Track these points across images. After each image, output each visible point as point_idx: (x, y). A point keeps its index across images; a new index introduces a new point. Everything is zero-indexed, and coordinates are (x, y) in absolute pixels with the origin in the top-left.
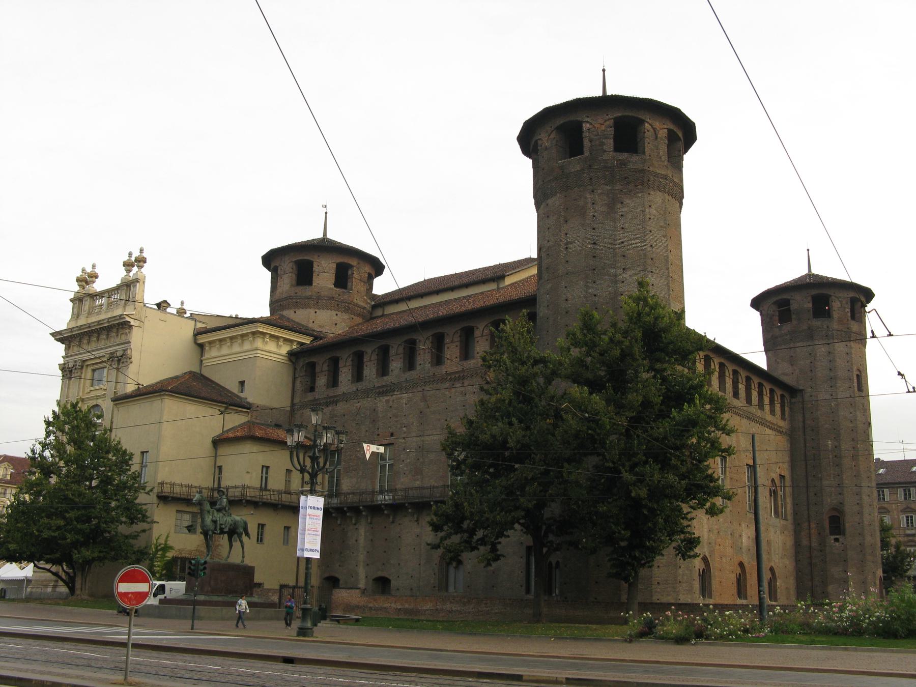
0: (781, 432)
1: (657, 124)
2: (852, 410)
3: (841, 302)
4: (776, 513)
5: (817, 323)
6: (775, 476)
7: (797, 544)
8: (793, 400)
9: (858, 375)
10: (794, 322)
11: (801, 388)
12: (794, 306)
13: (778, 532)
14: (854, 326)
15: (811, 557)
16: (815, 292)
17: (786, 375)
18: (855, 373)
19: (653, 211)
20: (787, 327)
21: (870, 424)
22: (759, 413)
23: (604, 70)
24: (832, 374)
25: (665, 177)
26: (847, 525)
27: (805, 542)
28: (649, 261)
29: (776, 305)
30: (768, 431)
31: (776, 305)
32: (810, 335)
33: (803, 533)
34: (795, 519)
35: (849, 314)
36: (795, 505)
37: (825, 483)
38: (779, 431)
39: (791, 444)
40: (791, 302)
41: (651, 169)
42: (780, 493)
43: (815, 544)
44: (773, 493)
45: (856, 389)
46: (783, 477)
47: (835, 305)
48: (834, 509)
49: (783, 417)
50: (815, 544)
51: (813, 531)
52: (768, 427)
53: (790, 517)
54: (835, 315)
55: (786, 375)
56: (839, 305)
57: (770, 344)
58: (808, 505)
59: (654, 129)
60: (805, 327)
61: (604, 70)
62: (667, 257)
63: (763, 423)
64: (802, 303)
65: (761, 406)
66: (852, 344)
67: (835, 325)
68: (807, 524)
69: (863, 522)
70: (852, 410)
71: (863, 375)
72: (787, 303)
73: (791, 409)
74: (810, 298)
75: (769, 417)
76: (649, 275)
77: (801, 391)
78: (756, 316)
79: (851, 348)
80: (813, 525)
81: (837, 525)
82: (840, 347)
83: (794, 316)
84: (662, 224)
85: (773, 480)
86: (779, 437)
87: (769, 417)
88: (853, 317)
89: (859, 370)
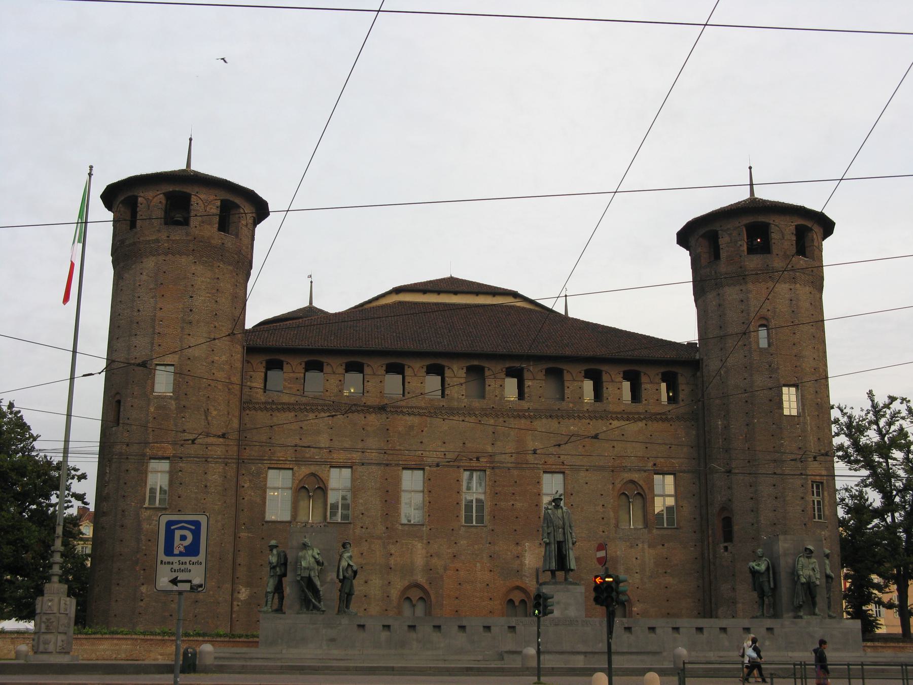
0: (667, 420)
1: (150, 194)
3: (730, 235)
6: (635, 476)
19: (144, 277)
23: (191, 139)
25: (157, 241)
28: (135, 325)
35: (745, 248)
41: (141, 239)
43: (711, 556)
47: (723, 241)
48: (723, 509)
52: (617, 419)
54: (723, 255)
59: (147, 200)
61: (191, 139)
62: (155, 316)
66: (750, 286)
70: (746, 375)
76: (133, 339)
80: (710, 532)
84: (151, 287)
85: (632, 482)
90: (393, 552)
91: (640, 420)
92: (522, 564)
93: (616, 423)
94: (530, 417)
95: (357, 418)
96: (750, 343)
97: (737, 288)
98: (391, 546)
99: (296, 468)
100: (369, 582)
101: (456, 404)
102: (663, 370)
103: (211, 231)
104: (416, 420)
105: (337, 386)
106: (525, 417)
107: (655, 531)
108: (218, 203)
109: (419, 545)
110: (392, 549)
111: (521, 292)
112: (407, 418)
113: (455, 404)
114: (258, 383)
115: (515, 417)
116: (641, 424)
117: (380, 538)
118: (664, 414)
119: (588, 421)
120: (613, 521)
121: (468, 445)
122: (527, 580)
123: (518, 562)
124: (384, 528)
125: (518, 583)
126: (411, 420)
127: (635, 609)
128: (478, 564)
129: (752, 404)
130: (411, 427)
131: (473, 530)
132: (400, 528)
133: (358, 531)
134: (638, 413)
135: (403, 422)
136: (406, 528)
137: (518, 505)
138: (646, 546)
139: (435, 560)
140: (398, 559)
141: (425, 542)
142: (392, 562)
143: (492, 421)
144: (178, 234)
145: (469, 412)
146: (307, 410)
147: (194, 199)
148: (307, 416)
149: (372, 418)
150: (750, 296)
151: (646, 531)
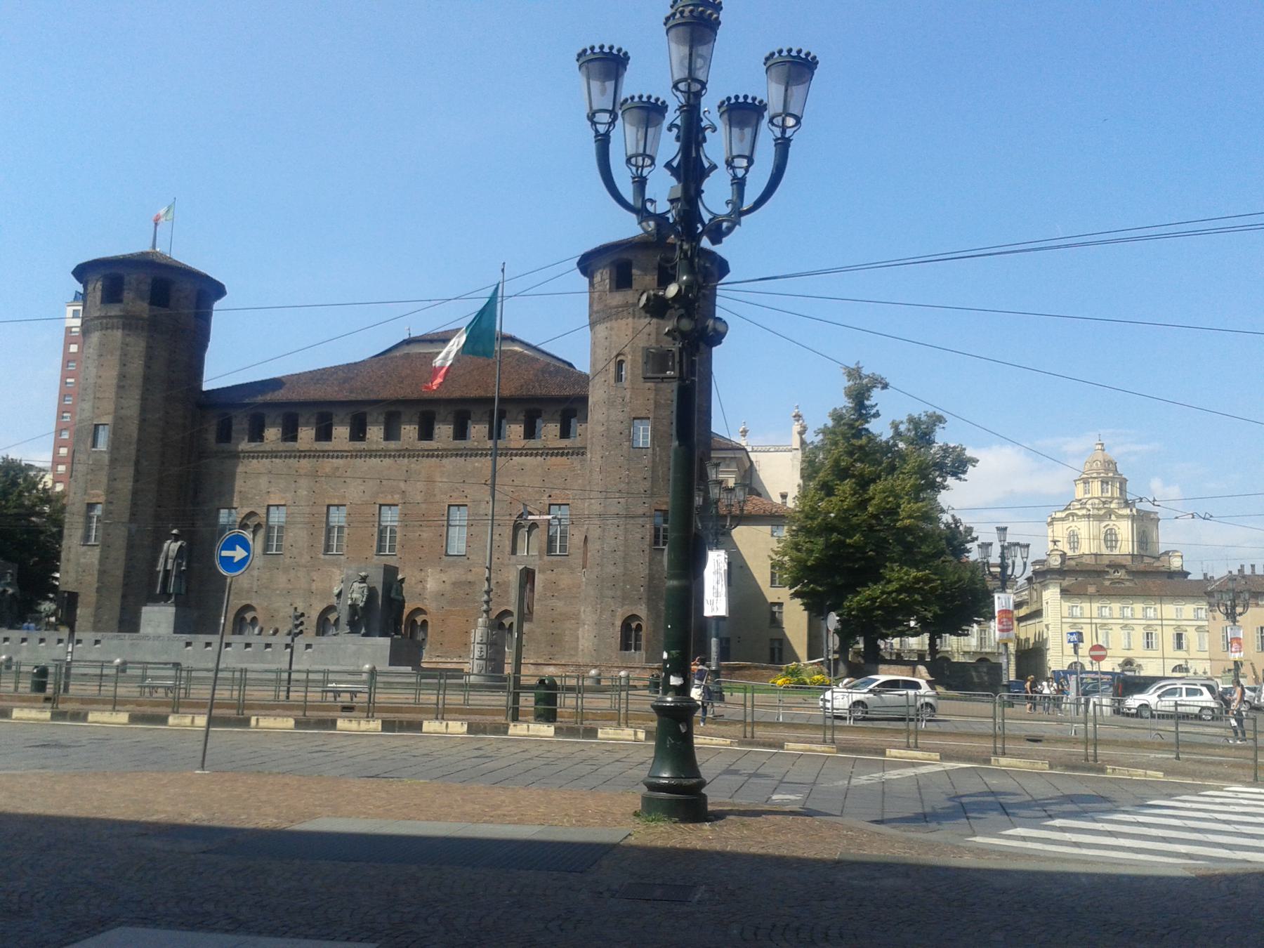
91: (537, 455)
92: (424, 588)
94: (438, 456)
103: (144, 308)
106: (433, 456)
107: (546, 558)
108: (149, 281)
110: (315, 575)
111: (518, 337)
112: (334, 460)
113: (374, 447)
114: (211, 437)
115: (428, 456)
120: (508, 549)
122: (427, 602)
123: (420, 586)
125: (420, 606)
126: (340, 462)
132: (322, 557)
133: (288, 561)
135: (328, 465)
137: (425, 535)
142: (314, 587)
143: (406, 460)
144: (115, 310)
145: (384, 454)
147: (127, 279)
149: (304, 462)
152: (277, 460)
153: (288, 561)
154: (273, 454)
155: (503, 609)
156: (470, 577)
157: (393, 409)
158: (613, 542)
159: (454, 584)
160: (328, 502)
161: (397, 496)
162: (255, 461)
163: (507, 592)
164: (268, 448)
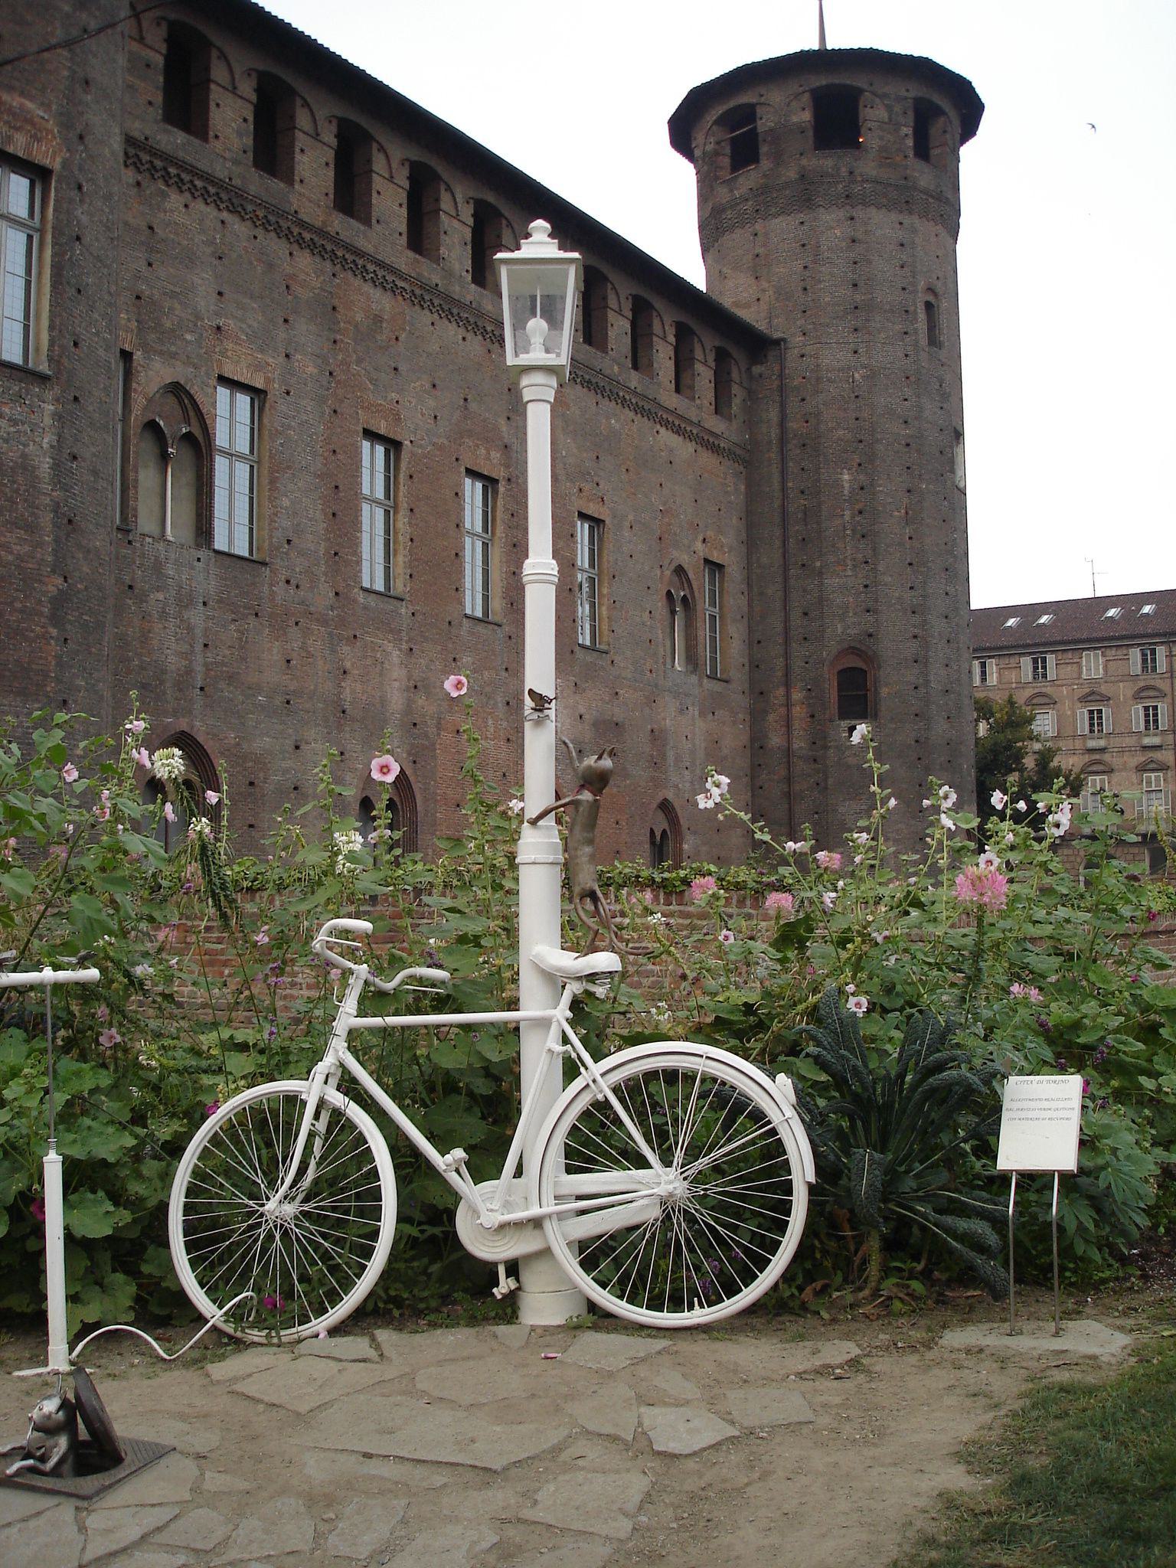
0: (715, 449)
2: (908, 392)
4: (692, 659)
5: (826, 162)
6: (685, 559)
7: (757, 745)
8: (757, 370)
9: (929, 306)
10: (765, 164)
11: (776, 335)
12: (766, 122)
13: (694, 711)
14: (924, 176)
15: (789, 780)
16: (821, 81)
17: (747, 305)
18: (922, 297)
20: (749, 179)
21: (958, 435)
22: (634, 380)
24: (858, 297)
26: (884, 691)
27: (776, 740)
29: (720, 122)
30: (666, 436)
31: (720, 122)
32: (807, 195)
33: (771, 717)
34: (752, 682)
35: (910, 142)
36: (754, 642)
37: (832, 582)
38: (708, 442)
39: (748, 486)
40: (759, 111)
42: (705, 607)
43: (799, 744)
44: (680, 603)
45: (923, 341)
46: (715, 567)
47: (874, 115)
49: (720, 406)
50: (799, 744)
51: (798, 711)
52: (666, 424)
53: (739, 676)
55: (747, 305)
56: (882, 118)
57: (713, 230)
58: (787, 642)
60: (792, 174)
63: (647, 409)
64: (787, 111)
65: (639, 357)
67: (868, 167)
68: (781, 691)
69: (928, 682)
71: (944, 304)
72: (748, 114)
73: (751, 394)
74: (806, 97)
75: (670, 399)
77: (777, 342)
78: (683, 174)
79: (914, 231)
80: (797, 695)
81: (856, 694)
82: (882, 224)
83: (764, 149)
85: (680, 570)
86: (707, 459)
87: (670, 399)
88: (922, 150)
89: (931, 290)
90: (348, 665)
93: (663, 430)
95: (278, 247)
96: (916, 331)
97: (894, 216)
98: (346, 649)
99: (138, 356)
100: (303, 747)
101: (457, 288)
102: (717, 343)
104: (383, 302)
105: (240, 135)
109: (395, 656)
113: (456, 290)
116: (691, 447)
117: (324, 622)
118: (717, 436)
119: (631, 414)
121: (473, 406)
124: (331, 595)
127: (685, 847)
128: (490, 722)
129: (918, 451)
130: (378, 319)
131: (480, 628)
132: (361, 597)
134: (691, 422)
136: (372, 601)
138: (697, 713)
139: (421, 701)
140: (359, 687)
141: (405, 646)
146: (166, 178)
148: (164, 195)
149: (305, 261)
150: (917, 240)
151: (694, 679)
152: (239, 228)
153: (280, 589)
154: (226, 196)
155: (660, 798)
156: (618, 713)
157: (491, 198)
158: (943, 672)
159: (596, 724)
160: (365, 419)
161: (496, 455)
162: (175, 200)
163: (664, 756)
164: (220, 171)
